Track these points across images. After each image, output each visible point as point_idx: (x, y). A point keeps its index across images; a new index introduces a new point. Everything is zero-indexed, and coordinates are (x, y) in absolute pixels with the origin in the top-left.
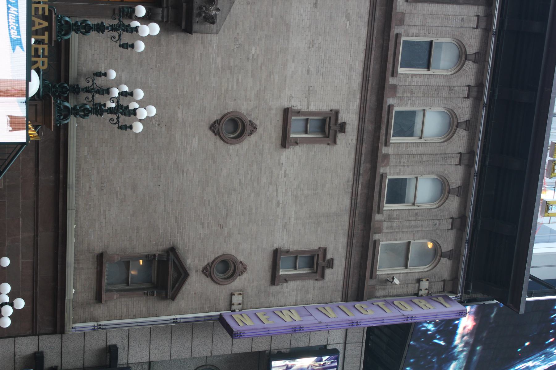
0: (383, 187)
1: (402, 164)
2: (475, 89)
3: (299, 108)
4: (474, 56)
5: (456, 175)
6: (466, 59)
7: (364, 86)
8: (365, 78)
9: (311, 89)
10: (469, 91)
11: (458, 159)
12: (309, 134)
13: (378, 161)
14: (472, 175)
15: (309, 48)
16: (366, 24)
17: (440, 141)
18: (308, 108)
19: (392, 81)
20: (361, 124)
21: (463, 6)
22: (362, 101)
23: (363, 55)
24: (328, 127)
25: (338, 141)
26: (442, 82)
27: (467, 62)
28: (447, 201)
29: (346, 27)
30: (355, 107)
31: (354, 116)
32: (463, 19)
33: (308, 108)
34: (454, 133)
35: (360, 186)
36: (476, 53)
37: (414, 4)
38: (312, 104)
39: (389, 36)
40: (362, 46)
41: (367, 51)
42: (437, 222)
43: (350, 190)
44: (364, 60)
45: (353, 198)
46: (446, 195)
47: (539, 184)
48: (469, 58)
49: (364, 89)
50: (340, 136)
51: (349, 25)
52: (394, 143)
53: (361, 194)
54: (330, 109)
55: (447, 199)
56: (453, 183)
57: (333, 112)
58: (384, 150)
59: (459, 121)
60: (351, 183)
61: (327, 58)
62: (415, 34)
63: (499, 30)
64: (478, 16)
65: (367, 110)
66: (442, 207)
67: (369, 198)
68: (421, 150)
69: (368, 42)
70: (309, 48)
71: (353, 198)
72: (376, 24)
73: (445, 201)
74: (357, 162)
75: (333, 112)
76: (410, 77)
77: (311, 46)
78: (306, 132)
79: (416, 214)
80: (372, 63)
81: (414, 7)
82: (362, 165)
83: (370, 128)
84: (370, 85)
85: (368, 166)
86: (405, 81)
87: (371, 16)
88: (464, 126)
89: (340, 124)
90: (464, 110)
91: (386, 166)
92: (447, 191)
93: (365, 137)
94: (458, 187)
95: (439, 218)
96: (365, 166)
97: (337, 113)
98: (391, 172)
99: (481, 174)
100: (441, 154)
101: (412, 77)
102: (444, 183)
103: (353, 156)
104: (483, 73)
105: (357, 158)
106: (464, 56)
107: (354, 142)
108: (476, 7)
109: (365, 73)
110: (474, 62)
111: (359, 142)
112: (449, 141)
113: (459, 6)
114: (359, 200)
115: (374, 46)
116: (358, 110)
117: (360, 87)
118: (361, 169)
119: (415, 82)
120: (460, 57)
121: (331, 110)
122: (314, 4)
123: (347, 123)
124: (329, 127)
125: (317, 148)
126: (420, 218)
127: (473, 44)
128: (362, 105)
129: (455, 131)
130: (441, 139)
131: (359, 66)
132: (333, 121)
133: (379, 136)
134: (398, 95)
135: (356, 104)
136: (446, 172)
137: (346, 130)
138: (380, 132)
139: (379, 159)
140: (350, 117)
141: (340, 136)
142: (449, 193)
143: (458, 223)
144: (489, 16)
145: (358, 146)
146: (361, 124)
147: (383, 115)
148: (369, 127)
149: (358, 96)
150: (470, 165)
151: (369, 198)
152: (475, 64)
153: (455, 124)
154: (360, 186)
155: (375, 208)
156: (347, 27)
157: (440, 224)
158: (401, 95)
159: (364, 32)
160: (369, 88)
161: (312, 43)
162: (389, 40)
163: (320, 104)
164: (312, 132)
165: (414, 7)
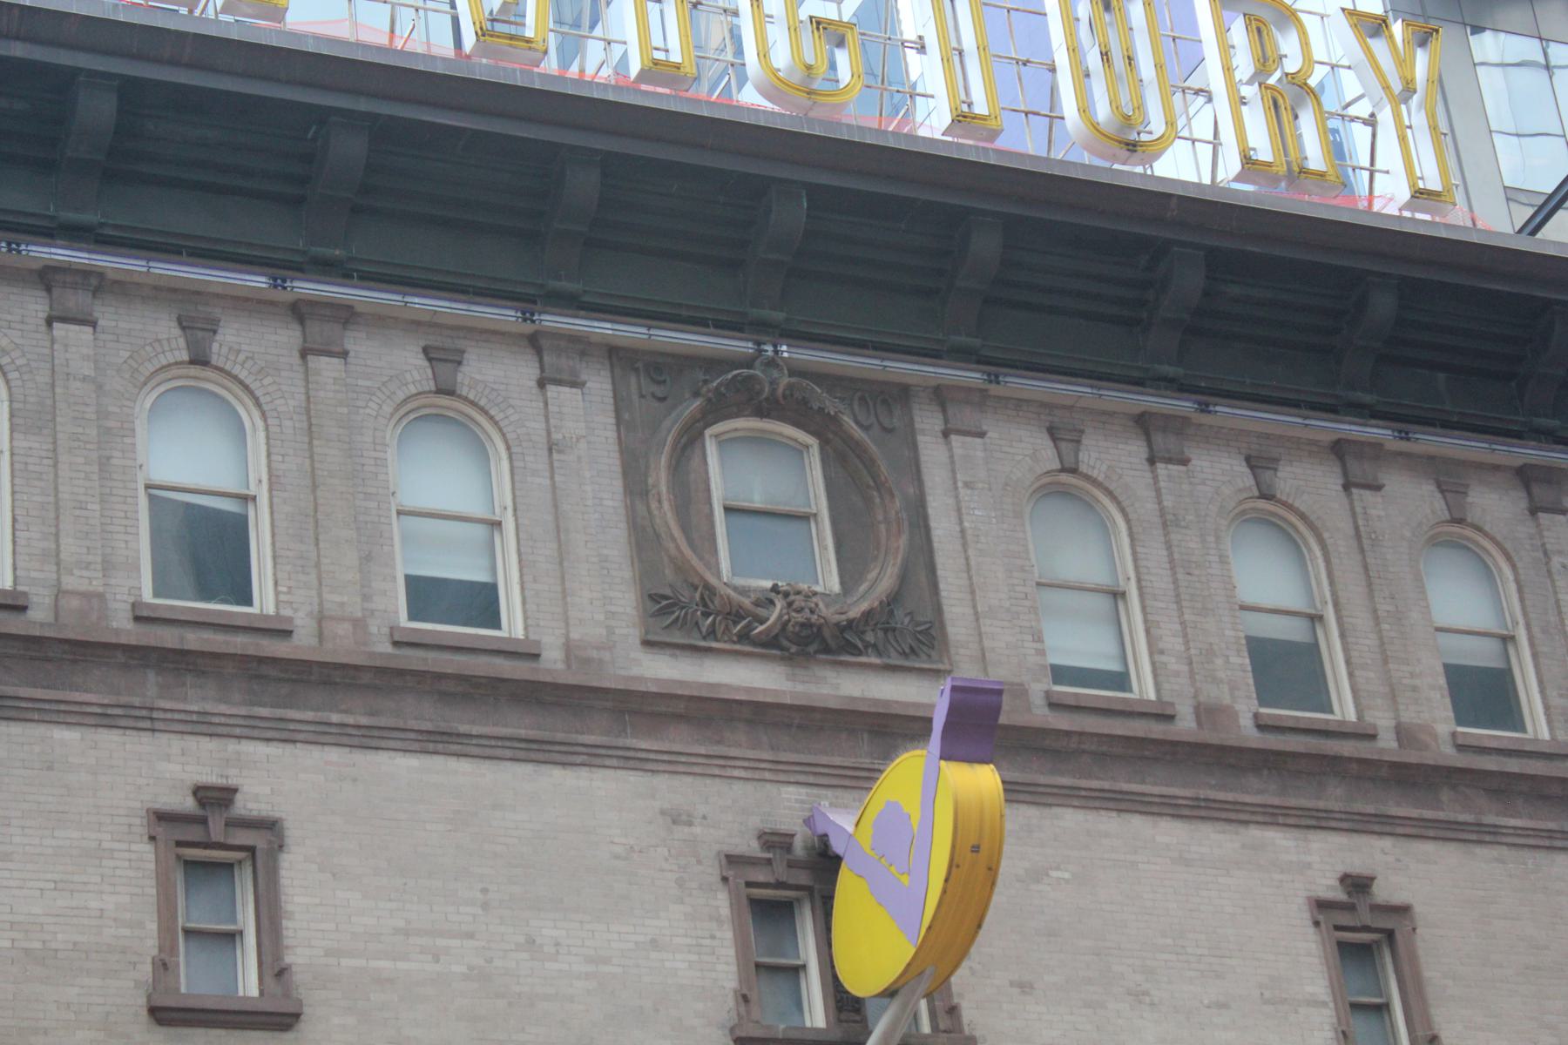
0: (1494, 744)
1: (1417, 682)
2: (1159, 439)
3: (1331, 1034)
4: (1063, 445)
5: (1407, 501)
6: (1074, 471)
7: (1224, 815)
8: (1203, 813)
9: (1267, 994)
10: (1169, 461)
11: (1367, 494)
12: (1389, 997)
13: (1431, 762)
14: (1404, 446)
15: (1152, 1004)
16: (1046, 811)
17: (1318, 553)
18: (1324, 1004)
19: (1186, 725)
20: (1333, 824)
21: (928, 484)
22: (1268, 819)
23: (1137, 823)
24: (1363, 936)
25: (1398, 898)
26: (1155, 553)
27: (1083, 468)
28: (1487, 528)
29: (1067, 881)
30: (1291, 843)
31: (1315, 846)
32: (967, 485)
33: (1324, 1004)
34: (1290, 507)
35: (1513, 822)
36: (1054, 439)
37: (953, 651)
38: (1309, 989)
39: (1068, 734)
40: (1109, 823)
41: (1123, 806)
42: (1556, 561)
43: (1526, 853)
44: (1150, 818)
45: (1547, 843)
46: (1469, 532)
47: (1444, 234)
48: (1069, 462)
49: (1233, 816)
50: (1384, 892)
51: (1058, 868)
52: (526, 628)
53: (1531, 818)
54: (1312, 930)
55: (1479, 529)
56: (1433, 512)
57: (1321, 918)
58: (1387, 743)
59: (1256, 493)
60: (1504, 850)
61: (1169, 941)
62: (1038, 645)
63: (978, 362)
64: (946, 434)
65: (1292, 802)
66: (1508, 546)
67: (1502, 788)
68: (1360, 619)
69: (1097, 804)
70: (1152, 1004)
71: (1547, 843)
72: (1042, 779)
73: (1486, 534)
74: (1441, 834)
75: (1321, 918)
76: (1164, 658)
77: (1147, 999)
78: (1382, 1009)
79: (1544, 631)
80: (1156, 790)
81: (962, 651)
82: (1441, 815)
83: (1339, 791)
84: (1221, 796)
85: (1446, 795)
86: (1177, 674)
87: (1021, 797)
88: (1267, 475)
89: (1349, 893)
90: (1217, 473)
91: (1435, 736)
92: (1455, 529)
93: (1370, 809)
94: (1442, 492)
95: (1540, 555)
96: (1450, 809)
97: (1322, 905)
98: (1438, 719)
99: (1403, 418)
100: (1362, 551)
101: (1162, 652)
102: (1244, 512)
103: (1429, 847)
104: (236, 298)
105: (1431, 833)
106: (1064, 477)
107: (1387, 843)
108: (920, 438)
109: (1186, 812)
110: (1078, 442)
111: (1388, 829)
112: (1318, 524)
113: (929, 498)
114: (1552, 825)
115: (1106, 785)
116: (1296, 833)
117: (1227, 827)
118: (1462, 818)
119: (1171, 641)
120: (1064, 493)
121: (1317, 924)
122: (1024, 992)
123: (1341, 868)
124: (1366, 929)
125: (1432, 972)
126: (1553, 619)
127: (1021, 450)
128: (1281, 820)
129: (1284, 504)
130: (1310, 550)
131: (1169, 833)
132: (1345, 919)
133: (1362, 761)
134: (1227, 700)
135: (1280, 841)
136: (1408, 534)
137: (1366, 872)
138: (1350, 759)
139: (1412, 757)
140: (1323, 860)
141: (1384, 892)
142: (1460, 521)
143: (1161, 440)
144: (941, 396)
145: (1400, 830)
146: (1333, 824)
147: (1302, 749)
148: (1334, 797)
149: (1255, 833)
150: (1375, 451)
151: (1502, 788)
152: (1085, 441)
153: (1262, 504)
154: (1513, 822)
155: (1156, 730)
156: (1067, 875)
157: (1560, 552)
158: (1225, 688)
159: (1071, 819)
160: (1230, 797)
161: (1138, 996)
162: (1081, 734)
163: (1307, 966)
164: (1381, 990)
165: (962, 651)
